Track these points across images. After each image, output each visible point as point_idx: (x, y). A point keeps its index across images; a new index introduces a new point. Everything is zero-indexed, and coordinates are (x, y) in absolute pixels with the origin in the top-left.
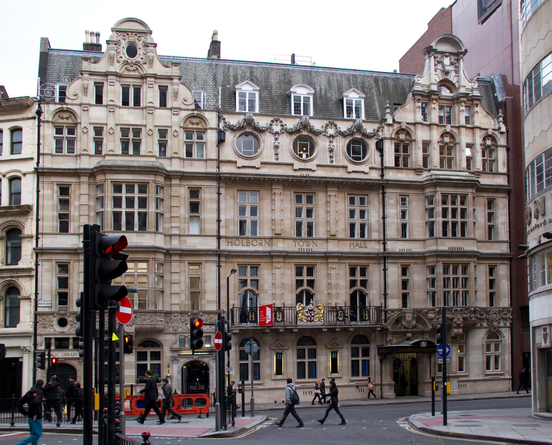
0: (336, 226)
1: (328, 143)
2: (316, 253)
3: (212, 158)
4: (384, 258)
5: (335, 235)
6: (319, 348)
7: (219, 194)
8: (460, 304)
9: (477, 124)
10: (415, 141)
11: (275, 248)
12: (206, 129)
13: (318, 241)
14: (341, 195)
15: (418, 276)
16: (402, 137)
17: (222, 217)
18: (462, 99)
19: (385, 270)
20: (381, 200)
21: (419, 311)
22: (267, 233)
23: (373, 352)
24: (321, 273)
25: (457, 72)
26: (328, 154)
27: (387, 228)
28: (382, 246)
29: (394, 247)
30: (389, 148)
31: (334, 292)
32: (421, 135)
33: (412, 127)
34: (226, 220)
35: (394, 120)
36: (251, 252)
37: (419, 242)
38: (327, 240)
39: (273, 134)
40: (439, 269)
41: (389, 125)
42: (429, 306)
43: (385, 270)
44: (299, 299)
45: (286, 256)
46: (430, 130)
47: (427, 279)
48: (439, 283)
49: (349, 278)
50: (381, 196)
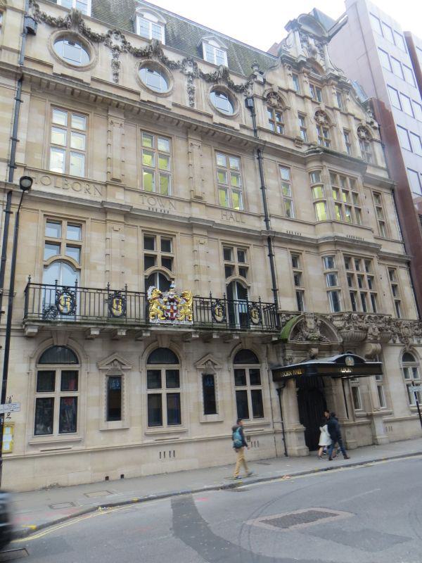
0: (203, 186)
1: (186, 83)
2: (170, 216)
3: (11, 46)
4: (269, 239)
5: (201, 198)
6: (184, 368)
7: (19, 100)
8: (370, 310)
9: (350, 111)
10: (289, 109)
11: (109, 200)
12: (5, 9)
13: (178, 203)
14: (206, 149)
15: (313, 268)
16: (274, 101)
17: (21, 136)
18: (332, 81)
19: (271, 255)
20: (257, 166)
21: (323, 316)
22: (100, 176)
23: (266, 377)
24: (182, 249)
25: (323, 56)
26: (187, 96)
27: (269, 202)
28: (264, 224)
29: (278, 226)
30: (260, 106)
31: (204, 278)
32: (294, 104)
33: (284, 93)
34: (28, 143)
35: (264, 80)
36: (70, 198)
37: (309, 227)
38: (190, 202)
39: (111, 48)
40: (340, 262)
41: (259, 83)
42: (331, 310)
43: (271, 255)
44: (149, 281)
45: (128, 215)
46: (304, 103)
47: (325, 274)
48: (342, 281)
49: (223, 262)
50: (257, 161)
